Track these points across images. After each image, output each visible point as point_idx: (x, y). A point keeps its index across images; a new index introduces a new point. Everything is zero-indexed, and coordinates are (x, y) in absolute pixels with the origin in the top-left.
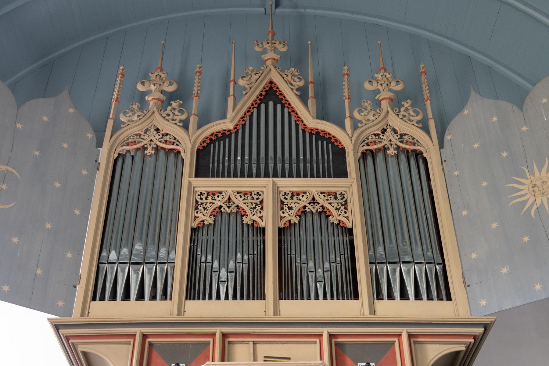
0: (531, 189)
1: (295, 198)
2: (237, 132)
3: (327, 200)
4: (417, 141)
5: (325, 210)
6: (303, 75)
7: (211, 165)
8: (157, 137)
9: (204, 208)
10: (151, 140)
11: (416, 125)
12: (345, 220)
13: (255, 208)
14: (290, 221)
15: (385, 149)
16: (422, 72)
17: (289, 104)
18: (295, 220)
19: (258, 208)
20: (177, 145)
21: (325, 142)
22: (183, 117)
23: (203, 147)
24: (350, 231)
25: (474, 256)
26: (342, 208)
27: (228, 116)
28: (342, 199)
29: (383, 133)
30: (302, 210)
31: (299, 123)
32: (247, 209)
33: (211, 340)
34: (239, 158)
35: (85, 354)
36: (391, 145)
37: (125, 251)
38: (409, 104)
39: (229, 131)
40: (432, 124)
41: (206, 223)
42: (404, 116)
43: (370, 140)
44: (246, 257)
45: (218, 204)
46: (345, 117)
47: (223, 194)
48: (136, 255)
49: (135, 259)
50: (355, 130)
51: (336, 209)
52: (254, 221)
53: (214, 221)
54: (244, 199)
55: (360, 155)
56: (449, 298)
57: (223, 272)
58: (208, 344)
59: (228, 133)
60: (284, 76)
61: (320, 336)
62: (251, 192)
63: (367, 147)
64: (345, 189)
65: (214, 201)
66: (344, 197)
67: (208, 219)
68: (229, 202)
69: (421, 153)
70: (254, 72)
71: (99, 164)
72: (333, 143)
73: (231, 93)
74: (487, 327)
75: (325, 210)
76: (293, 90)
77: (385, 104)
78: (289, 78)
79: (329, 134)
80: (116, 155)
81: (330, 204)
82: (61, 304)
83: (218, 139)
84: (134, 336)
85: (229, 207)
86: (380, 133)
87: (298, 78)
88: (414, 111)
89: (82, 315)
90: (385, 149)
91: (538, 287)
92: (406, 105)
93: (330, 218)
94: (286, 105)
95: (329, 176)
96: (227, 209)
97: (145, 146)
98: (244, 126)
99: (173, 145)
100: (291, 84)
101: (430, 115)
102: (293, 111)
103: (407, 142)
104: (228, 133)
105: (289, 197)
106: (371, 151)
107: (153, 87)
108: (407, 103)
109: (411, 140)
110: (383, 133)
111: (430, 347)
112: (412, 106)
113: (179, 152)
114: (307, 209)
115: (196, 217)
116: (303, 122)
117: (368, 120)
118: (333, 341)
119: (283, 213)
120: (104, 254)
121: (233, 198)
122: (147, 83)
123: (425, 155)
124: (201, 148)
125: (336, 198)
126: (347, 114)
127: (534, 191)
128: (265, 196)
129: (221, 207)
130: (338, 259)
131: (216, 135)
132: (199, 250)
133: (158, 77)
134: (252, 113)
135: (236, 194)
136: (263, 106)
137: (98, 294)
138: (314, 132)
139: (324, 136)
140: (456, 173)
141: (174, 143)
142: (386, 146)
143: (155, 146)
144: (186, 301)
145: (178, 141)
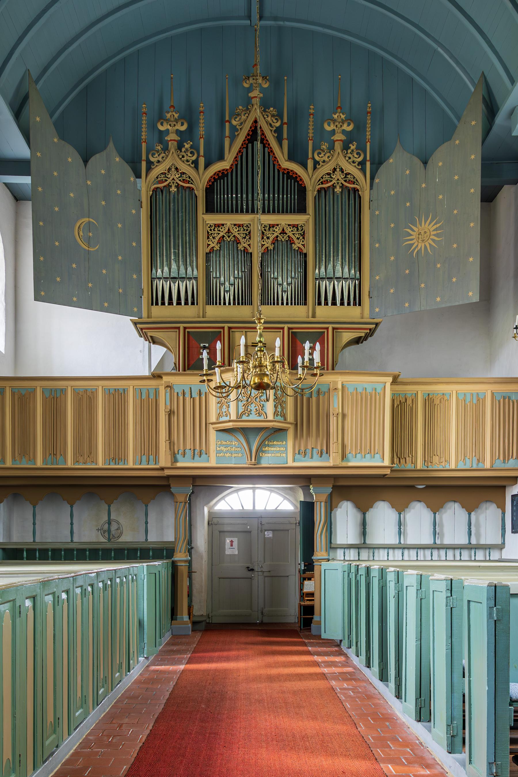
0: (417, 236)
1: (271, 229)
2: (232, 171)
3: (292, 231)
4: (357, 180)
5: (290, 239)
6: (280, 116)
7: (215, 201)
8: (177, 176)
9: (214, 238)
10: (173, 179)
11: (357, 167)
12: (302, 247)
13: (245, 238)
14: (267, 247)
15: (334, 186)
16: (368, 113)
17: (269, 145)
18: (271, 247)
19: (247, 238)
20: (192, 183)
21: (293, 181)
22: (194, 158)
23: (210, 185)
24: (305, 255)
25: (377, 278)
26: (301, 238)
27: (225, 159)
28: (301, 230)
29: (334, 172)
30: (275, 239)
31: (276, 163)
32: (240, 238)
33: (222, 330)
34: (234, 196)
35: (151, 337)
36: (338, 183)
37: (166, 269)
38: (355, 146)
39: (227, 170)
40: (368, 164)
41: (215, 249)
42: (350, 158)
43: (324, 179)
44: (240, 274)
45: (222, 234)
46: (308, 158)
47: (225, 226)
48: (173, 273)
49: (173, 275)
50: (314, 170)
51: (298, 239)
52: (245, 247)
53: (220, 248)
54: (238, 231)
55: (316, 192)
56: (360, 305)
57: (227, 284)
58: (221, 332)
59: (226, 173)
60: (265, 116)
61: (283, 328)
62: (243, 224)
63: (321, 186)
64: (304, 223)
65: (219, 232)
66: (303, 229)
67: (216, 246)
68: (229, 233)
69: (358, 190)
70: (243, 113)
71: (141, 202)
72: (298, 182)
73: (227, 134)
74: (377, 324)
75: (290, 239)
76: (271, 131)
77: (338, 146)
78: (269, 119)
79: (296, 174)
80: (151, 193)
81: (293, 234)
82: (135, 309)
83: (220, 178)
84: (179, 328)
85: (229, 237)
86: (331, 172)
87: (276, 119)
88: (357, 154)
89: (148, 317)
90: (334, 186)
91: (407, 305)
92: (353, 147)
93: (293, 245)
94: (267, 146)
95: (294, 212)
96: (228, 238)
97: (170, 184)
98: (237, 165)
99: (189, 183)
100: (271, 125)
101: (368, 158)
102: (272, 151)
103: (349, 183)
104: (226, 173)
105: (267, 229)
106: (324, 188)
107: (169, 127)
108: (353, 145)
109: (352, 179)
110: (334, 172)
111: (344, 333)
112: (357, 149)
113: (193, 189)
114: (279, 239)
115: (209, 245)
116: (278, 162)
117: (324, 161)
118: (291, 331)
119: (263, 241)
120: (154, 271)
121: (231, 230)
122: (165, 124)
123: (360, 193)
124: (208, 187)
125: (298, 229)
126: (310, 156)
127: (418, 238)
128: (252, 228)
129: (223, 236)
130: (297, 275)
131: (218, 174)
132: (211, 268)
133: (172, 116)
134: (242, 153)
135: (233, 226)
136: (250, 145)
137: (154, 302)
138: (286, 172)
139: (292, 176)
140: (377, 213)
141: (189, 181)
142: (335, 185)
143: (177, 185)
144: (207, 306)
145: (192, 180)
